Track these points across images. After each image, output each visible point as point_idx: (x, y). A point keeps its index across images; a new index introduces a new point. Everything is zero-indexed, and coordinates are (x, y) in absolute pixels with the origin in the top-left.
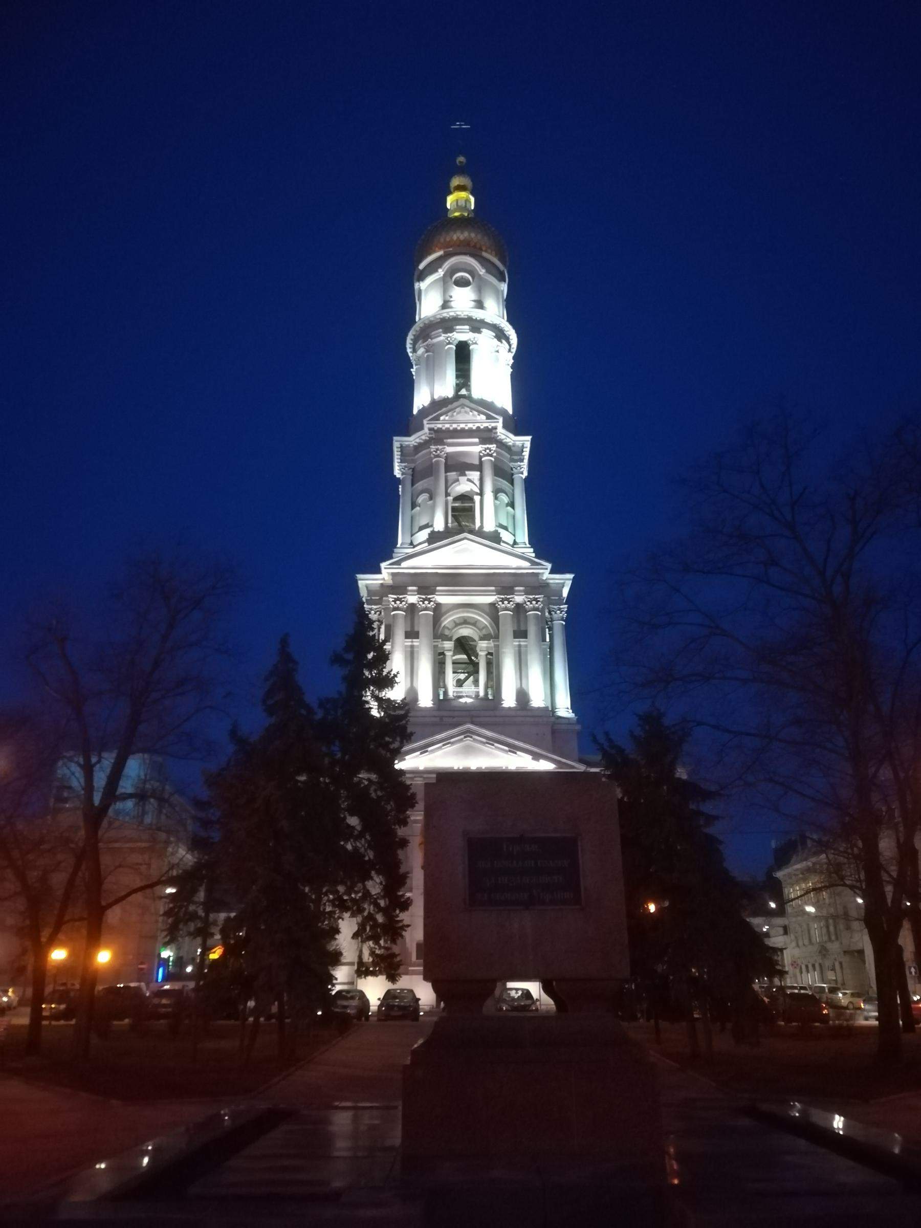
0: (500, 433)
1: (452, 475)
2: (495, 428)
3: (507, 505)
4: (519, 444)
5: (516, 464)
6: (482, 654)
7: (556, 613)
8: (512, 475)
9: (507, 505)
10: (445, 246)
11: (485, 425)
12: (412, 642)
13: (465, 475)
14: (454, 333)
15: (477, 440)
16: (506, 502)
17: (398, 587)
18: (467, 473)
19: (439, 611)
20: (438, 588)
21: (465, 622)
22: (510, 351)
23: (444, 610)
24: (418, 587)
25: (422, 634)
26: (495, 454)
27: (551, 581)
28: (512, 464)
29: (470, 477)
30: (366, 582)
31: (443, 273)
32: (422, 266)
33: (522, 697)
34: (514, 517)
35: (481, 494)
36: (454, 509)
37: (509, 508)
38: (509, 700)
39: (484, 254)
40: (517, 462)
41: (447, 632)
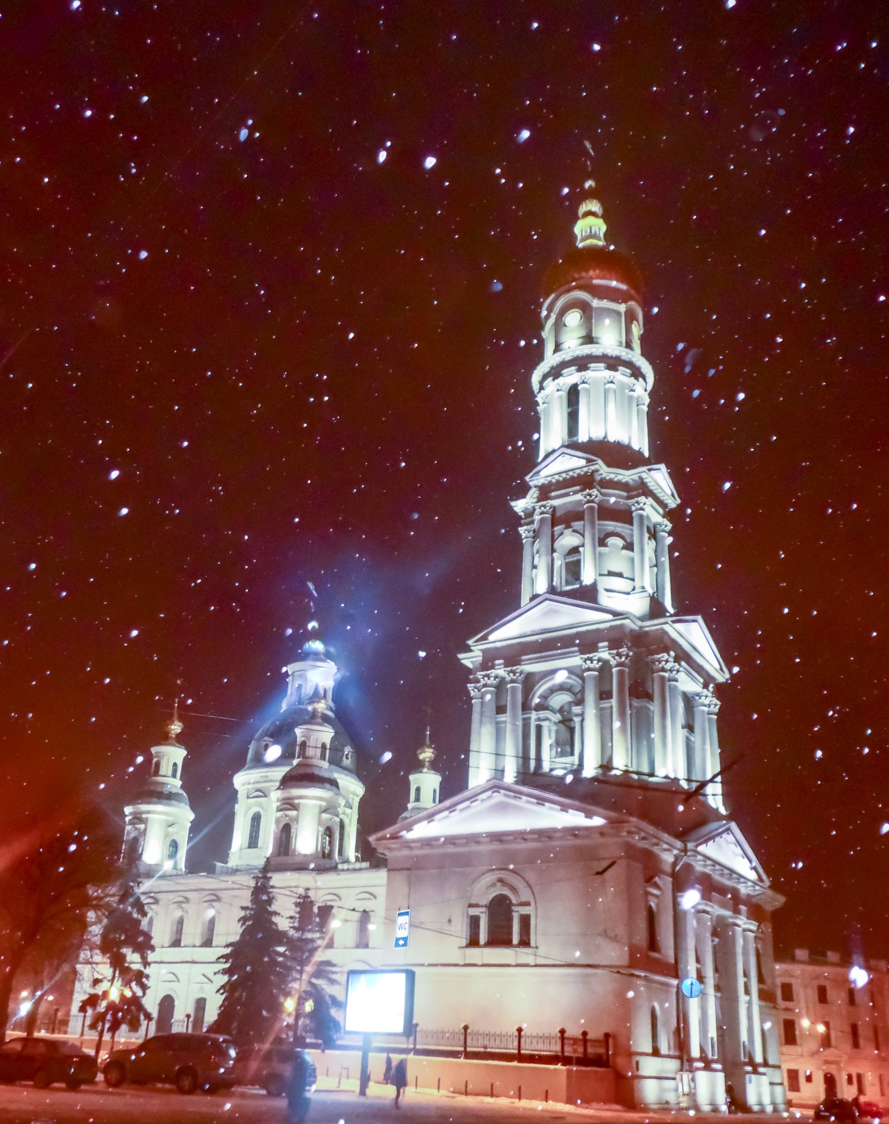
0: (606, 472)
1: (558, 529)
3: (624, 548)
4: (636, 477)
7: (655, 664)
8: (632, 512)
9: (624, 548)
11: (585, 469)
13: (571, 527)
14: (561, 378)
15: (578, 488)
16: (622, 545)
18: (573, 524)
19: (530, 682)
20: (524, 657)
22: (637, 373)
23: (537, 678)
24: (504, 659)
31: (555, 316)
34: (632, 560)
35: (583, 546)
37: (625, 552)
39: (596, 282)
40: (634, 498)
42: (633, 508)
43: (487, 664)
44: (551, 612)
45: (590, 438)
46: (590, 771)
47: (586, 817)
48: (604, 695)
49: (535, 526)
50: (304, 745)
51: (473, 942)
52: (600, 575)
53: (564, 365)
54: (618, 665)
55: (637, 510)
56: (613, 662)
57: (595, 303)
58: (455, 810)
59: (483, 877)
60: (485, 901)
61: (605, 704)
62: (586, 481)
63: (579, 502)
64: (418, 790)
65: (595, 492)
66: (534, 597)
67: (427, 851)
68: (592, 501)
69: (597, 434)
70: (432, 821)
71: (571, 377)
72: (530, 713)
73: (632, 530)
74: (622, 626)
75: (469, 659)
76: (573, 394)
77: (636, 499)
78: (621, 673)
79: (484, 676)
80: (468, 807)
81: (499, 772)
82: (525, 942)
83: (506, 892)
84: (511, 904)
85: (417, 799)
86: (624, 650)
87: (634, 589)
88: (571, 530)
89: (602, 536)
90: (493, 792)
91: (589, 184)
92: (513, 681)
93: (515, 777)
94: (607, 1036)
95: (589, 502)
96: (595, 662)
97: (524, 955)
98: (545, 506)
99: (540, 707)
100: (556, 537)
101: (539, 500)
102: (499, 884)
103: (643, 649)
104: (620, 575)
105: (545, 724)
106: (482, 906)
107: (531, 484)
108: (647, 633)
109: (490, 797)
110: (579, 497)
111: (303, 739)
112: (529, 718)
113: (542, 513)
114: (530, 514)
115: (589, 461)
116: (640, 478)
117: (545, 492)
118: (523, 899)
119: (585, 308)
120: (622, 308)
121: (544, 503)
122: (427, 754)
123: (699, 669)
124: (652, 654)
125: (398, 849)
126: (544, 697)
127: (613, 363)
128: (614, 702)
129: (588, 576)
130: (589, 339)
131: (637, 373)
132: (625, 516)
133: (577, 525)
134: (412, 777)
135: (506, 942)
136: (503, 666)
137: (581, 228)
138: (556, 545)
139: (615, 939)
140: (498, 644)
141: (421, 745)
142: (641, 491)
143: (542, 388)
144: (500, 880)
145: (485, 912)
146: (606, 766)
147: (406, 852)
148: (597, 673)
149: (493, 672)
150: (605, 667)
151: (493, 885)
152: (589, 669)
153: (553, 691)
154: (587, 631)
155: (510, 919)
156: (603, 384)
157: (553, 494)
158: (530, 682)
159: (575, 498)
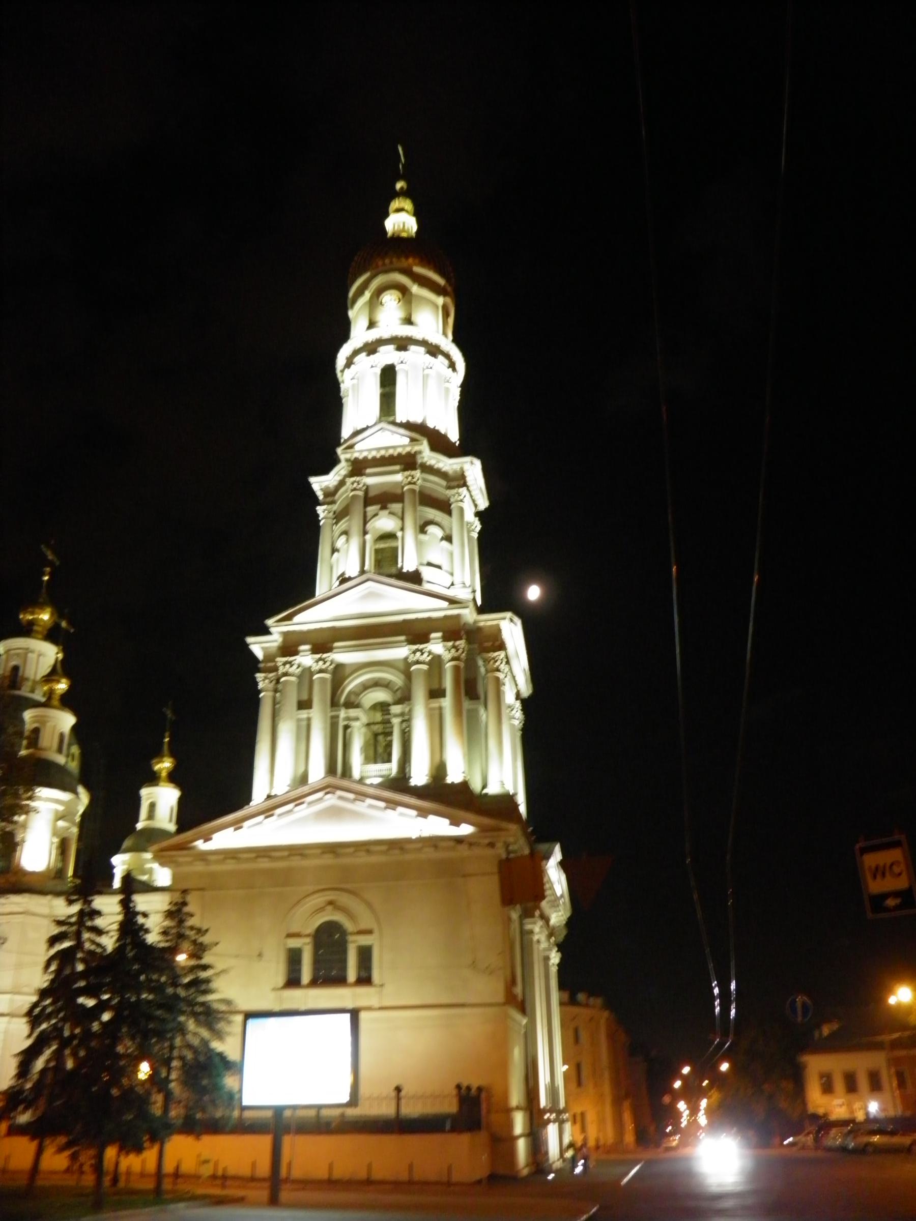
1: (371, 509)
2: (420, 452)
3: (442, 539)
4: (457, 467)
5: (455, 491)
6: (396, 721)
8: (450, 505)
9: (442, 539)
11: (408, 449)
12: (308, 713)
15: (397, 467)
19: (339, 674)
20: (336, 644)
21: (376, 684)
22: (452, 366)
23: (348, 671)
26: (419, 482)
27: (482, 624)
28: (449, 493)
29: (392, 510)
30: (258, 646)
32: (351, 294)
33: (439, 771)
34: (451, 554)
35: (402, 529)
36: (377, 551)
37: (445, 544)
38: (419, 776)
41: (353, 698)
42: (452, 500)
43: (289, 648)
44: (371, 595)
47: (451, 824)
48: (436, 693)
49: (335, 507)
50: (36, 731)
51: (293, 981)
52: (422, 564)
53: (381, 342)
54: (453, 659)
55: (457, 501)
57: (415, 289)
58: (272, 815)
59: (307, 900)
60: (312, 927)
61: (435, 704)
62: (408, 462)
64: (152, 806)
66: (343, 580)
67: (230, 866)
68: (414, 483)
69: (417, 419)
70: (241, 827)
71: (387, 355)
72: (340, 710)
73: (451, 523)
74: (458, 617)
75: (258, 646)
76: (388, 376)
77: (457, 489)
78: (456, 669)
79: (285, 664)
80: (290, 811)
81: (303, 779)
82: (365, 980)
83: (337, 917)
84: (344, 933)
85: (151, 816)
86: (461, 643)
87: (452, 584)
88: (386, 512)
89: (422, 523)
90: (327, 793)
91: (399, 185)
92: (321, 671)
94: (480, 1089)
95: (410, 483)
96: (426, 655)
98: (358, 483)
99: (349, 705)
100: (368, 518)
101: (352, 474)
102: (330, 908)
103: (476, 646)
104: (439, 567)
105: (356, 724)
106: (308, 936)
107: (342, 457)
108: (479, 629)
109: (320, 799)
110: (399, 477)
111: (35, 725)
112: (338, 717)
113: (355, 489)
114: (330, 494)
115: (413, 440)
116: (462, 469)
117: (358, 467)
118: (363, 926)
119: (403, 290)
120: (440, 300)
121: (358, 479)
122: (165, 765)
124: (489, 652)
125: (190, 863)
126: (357, 693)
127: (434, 350)
128: (447, 703)
129: (409, 563)
130: (408, 321)
131: (452, 366)
132: (445, 507)
133: (396, 507)
134: (145, 792)
135: (340, 980)
136: (310, 652)
138: (369, 526)
139: (490, 971)
140: (305, 628)
141: (158, 754)
142: (462, 482)
143: (349, 363)
144: (331, 903)
145: (309, 943)
147: (199, 867)
148: (425, 667)
149: (298, 659)
150: (436, 662)
151: (321, 909)
152: (418, 662)
153: (366, 687)
154: (417, 620)
155: (344, 952)
156: (422, 370)
157: (368, 471)
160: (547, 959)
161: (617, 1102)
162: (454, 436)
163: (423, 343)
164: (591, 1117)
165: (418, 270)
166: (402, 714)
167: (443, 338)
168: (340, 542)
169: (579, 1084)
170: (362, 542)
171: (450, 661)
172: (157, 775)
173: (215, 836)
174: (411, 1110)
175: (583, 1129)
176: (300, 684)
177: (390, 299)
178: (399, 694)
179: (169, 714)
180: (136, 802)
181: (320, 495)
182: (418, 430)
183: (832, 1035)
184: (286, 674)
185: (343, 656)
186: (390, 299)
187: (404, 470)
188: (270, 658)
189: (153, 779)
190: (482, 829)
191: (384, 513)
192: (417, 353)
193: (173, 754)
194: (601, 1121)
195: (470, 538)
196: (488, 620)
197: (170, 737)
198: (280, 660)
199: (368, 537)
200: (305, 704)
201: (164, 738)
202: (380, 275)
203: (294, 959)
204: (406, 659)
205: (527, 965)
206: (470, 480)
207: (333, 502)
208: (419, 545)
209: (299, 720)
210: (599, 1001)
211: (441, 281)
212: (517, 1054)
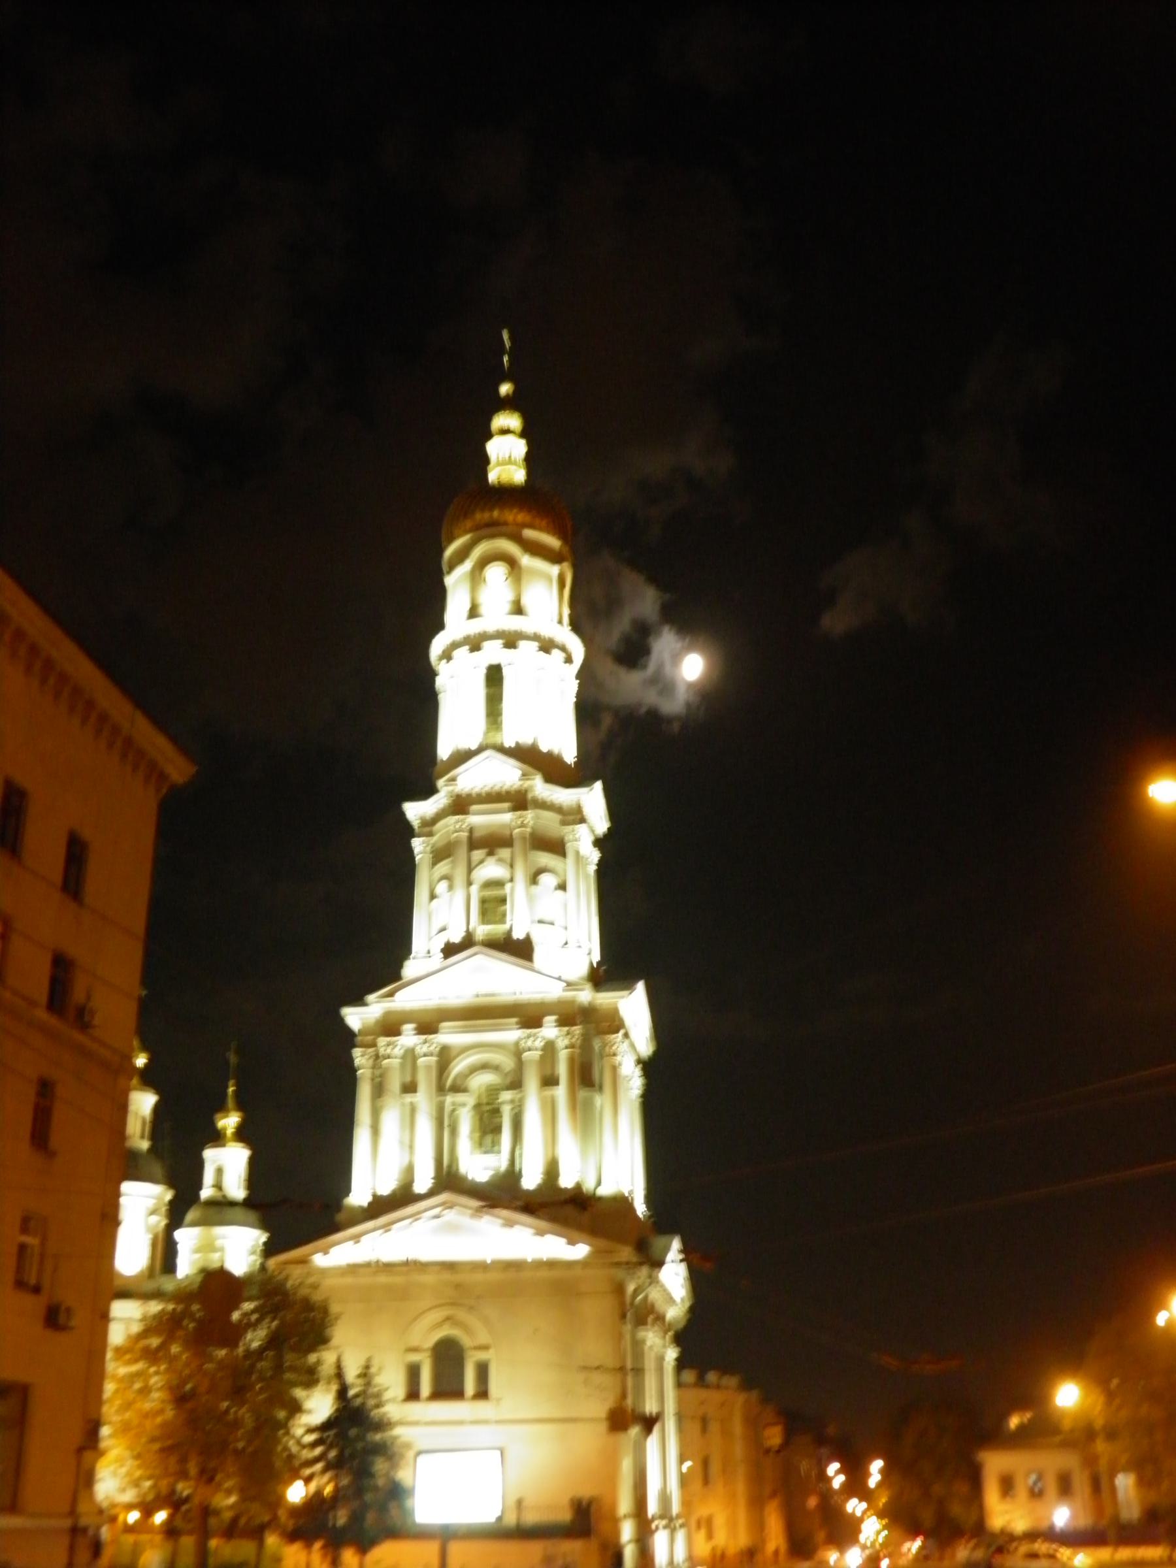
1: (478, 854)
5: (570, 827)
10: (477, 528)
15: (506, 805)
17: (390, 1027)
21: (484, 1067)
22: (569, 660)
23: (453, 1053)
25: (422, 1086)
30: (354, 1017)
32: (449, 552)
34: (565, 905)
35: (511, 880)
36: (483, 901)
37: (560, 893)
39: (529, 534)
41: (459, 1082)
42: (566, 838)
45: (517, 743)
46: (531, 1180)
48: (549, 1081)
52: (533, 922)
53: (485, 637)
54: (571, 1046)
56: (562, 1043)
57: (526, 560)
62: (519, 801)
63: (504, 826)
64: (219, 1171)
65: (529, 816)
69: (526, 740)
71: (493, 652)
75: (354, 1017)
76: (494, 676)
78: (571, 1060)
82: (482, 1394)
86: (577, 1030)
91: (505, 389)
92: (425, 1055)
93: (432, 1178)
97: (481, 1409)
99: (457, 1088)
100: (473, 864)
104: (552, 924)
114: (429, 824)
115: (525, 775)
117: (460, 805)
119: (512, 563)
120: (554, 570)
122: (229, 1122)
123: (633, 1046)
127: (547, 646)
128: (561, 1092)
130: (518, 609)
131: (569, 660)
132: (557, 847)
137: (496, 448)
143: (447, 655)
144: (448, 1318)
146: (552, 1171)
151: (439, 1325)
157: (474, 808)
158: (445, 1057)
159: (504, 818)
160: (661, 1359)
161: (756, 1503)
162: (570, 755)
163: (535, 637)
164: (720, 1521)
165: (529, 534)
166: (512, 1101)
167: (559, 626)
168: (442, 887)
169: (706, 1480)
170: (465, 897)
171: (563, 1049)
172: (222, 1132)
173: (333, 1250)
174: (531, 1518)
175: (710, 1536)
176: (403, 1065)
177: (496, 573)
178: (508, 1081)
179: (233, 1059)
180: (199, 1165)
181: (416, 823)
182: (528, 756)
183: (1021, 1428)
184: (389, 1057)
185: (450, 1036)
186: (496, 573)
187: (515, 809)
188: (364, 1032)
189: (216, 1138)
190: (596, 1253)
191: (491, 861)
192: (527, 648)
193: (241, 1106)
194: (732, 1525)
195: (587, 876)
196: (605, 999)
197: (237, 1085)
198: (382, 1041)
199: (474, 889)
200: (410, 1088)
201: (227, 1087)
202: (484, 540)
203: (413, 1373)
204: (517, 1044)
205: (639, 1371)
206: (587, 811)
207: (430, 834)
208: (531, 899)
209: (403, 1105)
210: (732, 1381)
211: (552, 541)
212: (626, 1465)
